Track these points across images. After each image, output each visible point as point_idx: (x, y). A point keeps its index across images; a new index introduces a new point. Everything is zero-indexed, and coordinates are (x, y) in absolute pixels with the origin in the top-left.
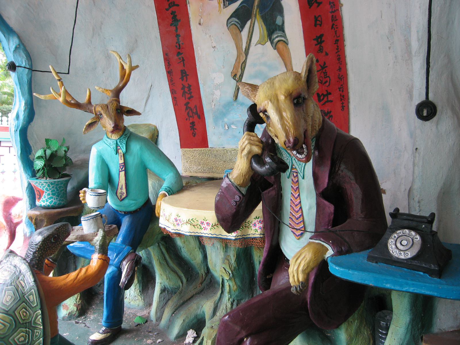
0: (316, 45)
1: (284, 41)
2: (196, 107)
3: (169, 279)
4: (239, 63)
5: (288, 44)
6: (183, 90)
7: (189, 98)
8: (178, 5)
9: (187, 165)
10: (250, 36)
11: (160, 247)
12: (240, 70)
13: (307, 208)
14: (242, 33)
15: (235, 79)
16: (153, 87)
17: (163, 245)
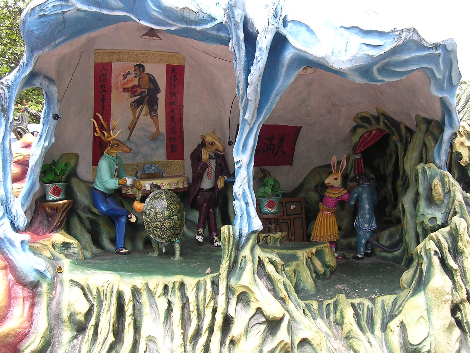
12: (133, 126)
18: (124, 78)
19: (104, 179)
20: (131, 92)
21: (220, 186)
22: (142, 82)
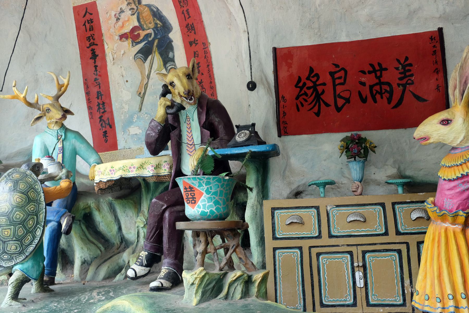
3: (90, 249)
4: (143, 84)
6: (98, 107)
7: (103, 113)
8: (97, 45)
10: (151, 66)
11: (81, 225)
13: (196, 137)
14: (145, 64)
15: (140, 96)
16: (72, 106)
17: (83, 223)
18: (117, 20)
20: (130, 38)
22: (143, 19)
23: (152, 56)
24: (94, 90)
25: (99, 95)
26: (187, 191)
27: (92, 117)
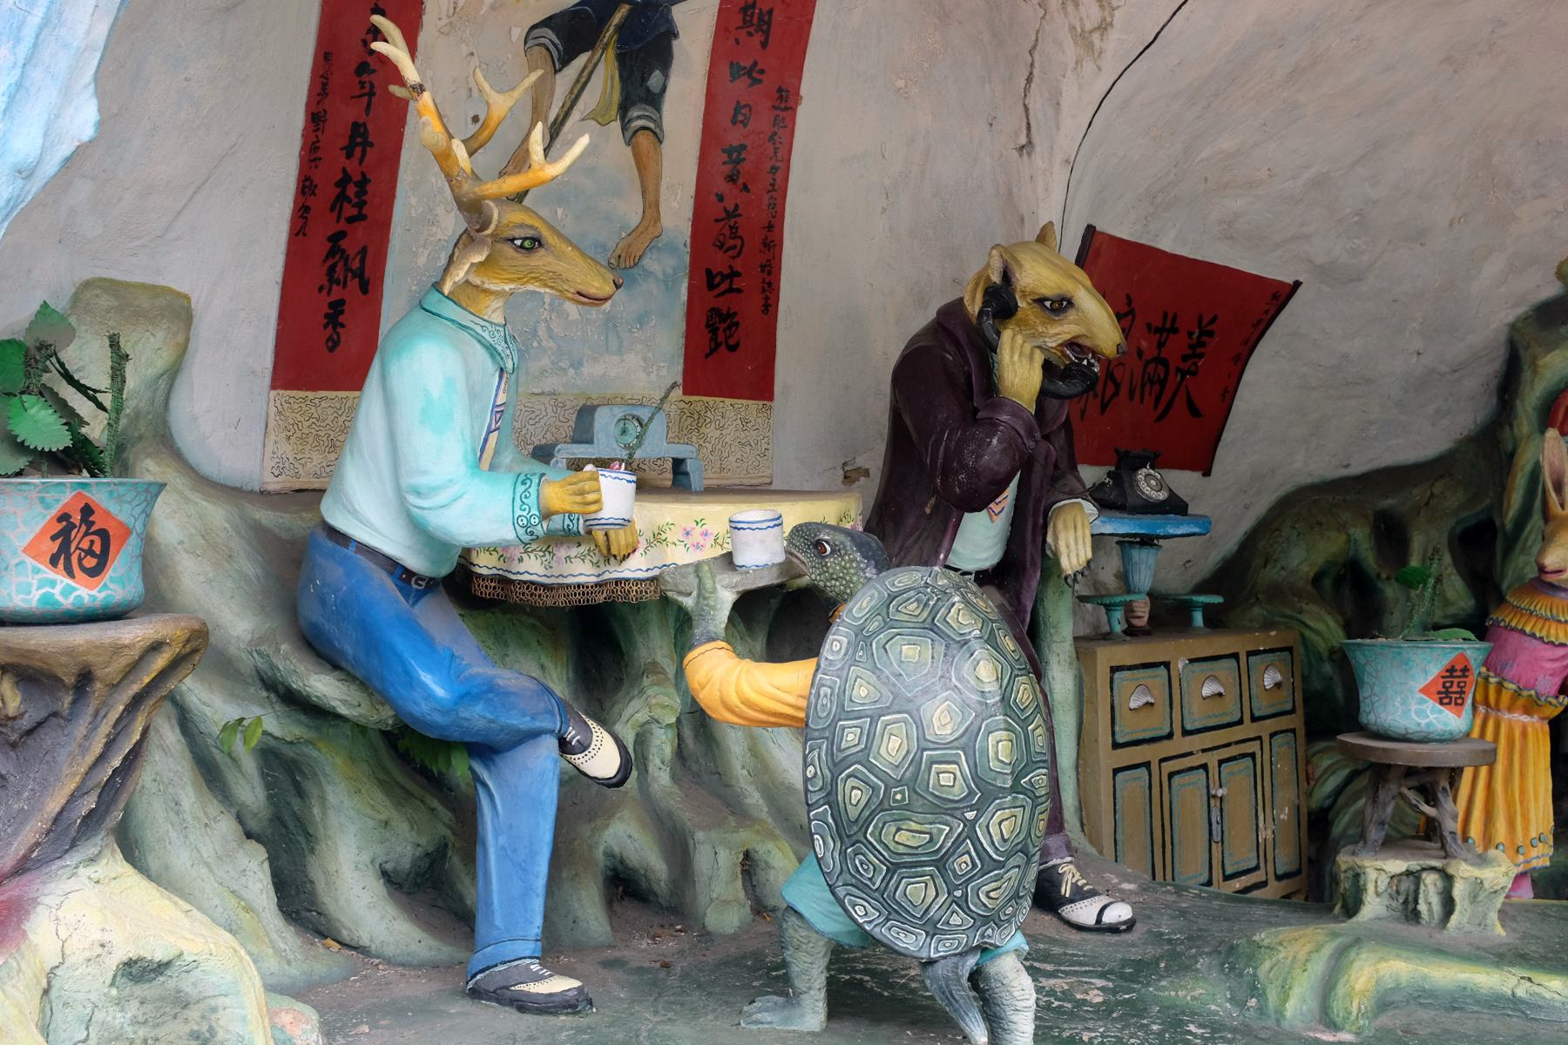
0: (724, 163)
1: (655, 133)
2: (364, 251)
5: (661, 142)
6: (339, 190)
7: (351, 220)
9: (287, 449)
10: (575, 91)
14: (558, 76)
19: (425, 473)
21: (1074, 561)
23: (592, 56)
24: (345, 114)
25: (359, 140)
26: (1452, 676)
27: (304, 226)
